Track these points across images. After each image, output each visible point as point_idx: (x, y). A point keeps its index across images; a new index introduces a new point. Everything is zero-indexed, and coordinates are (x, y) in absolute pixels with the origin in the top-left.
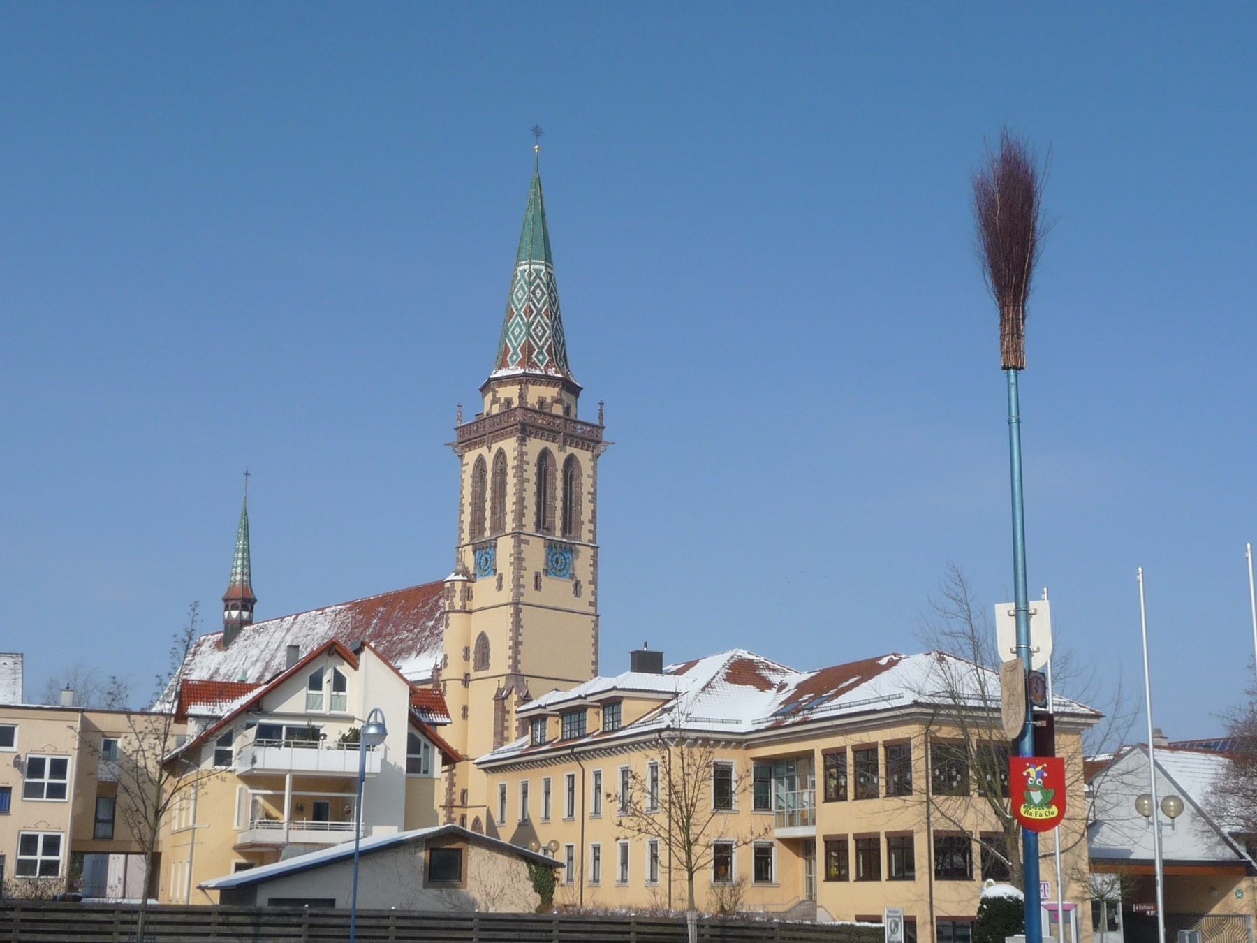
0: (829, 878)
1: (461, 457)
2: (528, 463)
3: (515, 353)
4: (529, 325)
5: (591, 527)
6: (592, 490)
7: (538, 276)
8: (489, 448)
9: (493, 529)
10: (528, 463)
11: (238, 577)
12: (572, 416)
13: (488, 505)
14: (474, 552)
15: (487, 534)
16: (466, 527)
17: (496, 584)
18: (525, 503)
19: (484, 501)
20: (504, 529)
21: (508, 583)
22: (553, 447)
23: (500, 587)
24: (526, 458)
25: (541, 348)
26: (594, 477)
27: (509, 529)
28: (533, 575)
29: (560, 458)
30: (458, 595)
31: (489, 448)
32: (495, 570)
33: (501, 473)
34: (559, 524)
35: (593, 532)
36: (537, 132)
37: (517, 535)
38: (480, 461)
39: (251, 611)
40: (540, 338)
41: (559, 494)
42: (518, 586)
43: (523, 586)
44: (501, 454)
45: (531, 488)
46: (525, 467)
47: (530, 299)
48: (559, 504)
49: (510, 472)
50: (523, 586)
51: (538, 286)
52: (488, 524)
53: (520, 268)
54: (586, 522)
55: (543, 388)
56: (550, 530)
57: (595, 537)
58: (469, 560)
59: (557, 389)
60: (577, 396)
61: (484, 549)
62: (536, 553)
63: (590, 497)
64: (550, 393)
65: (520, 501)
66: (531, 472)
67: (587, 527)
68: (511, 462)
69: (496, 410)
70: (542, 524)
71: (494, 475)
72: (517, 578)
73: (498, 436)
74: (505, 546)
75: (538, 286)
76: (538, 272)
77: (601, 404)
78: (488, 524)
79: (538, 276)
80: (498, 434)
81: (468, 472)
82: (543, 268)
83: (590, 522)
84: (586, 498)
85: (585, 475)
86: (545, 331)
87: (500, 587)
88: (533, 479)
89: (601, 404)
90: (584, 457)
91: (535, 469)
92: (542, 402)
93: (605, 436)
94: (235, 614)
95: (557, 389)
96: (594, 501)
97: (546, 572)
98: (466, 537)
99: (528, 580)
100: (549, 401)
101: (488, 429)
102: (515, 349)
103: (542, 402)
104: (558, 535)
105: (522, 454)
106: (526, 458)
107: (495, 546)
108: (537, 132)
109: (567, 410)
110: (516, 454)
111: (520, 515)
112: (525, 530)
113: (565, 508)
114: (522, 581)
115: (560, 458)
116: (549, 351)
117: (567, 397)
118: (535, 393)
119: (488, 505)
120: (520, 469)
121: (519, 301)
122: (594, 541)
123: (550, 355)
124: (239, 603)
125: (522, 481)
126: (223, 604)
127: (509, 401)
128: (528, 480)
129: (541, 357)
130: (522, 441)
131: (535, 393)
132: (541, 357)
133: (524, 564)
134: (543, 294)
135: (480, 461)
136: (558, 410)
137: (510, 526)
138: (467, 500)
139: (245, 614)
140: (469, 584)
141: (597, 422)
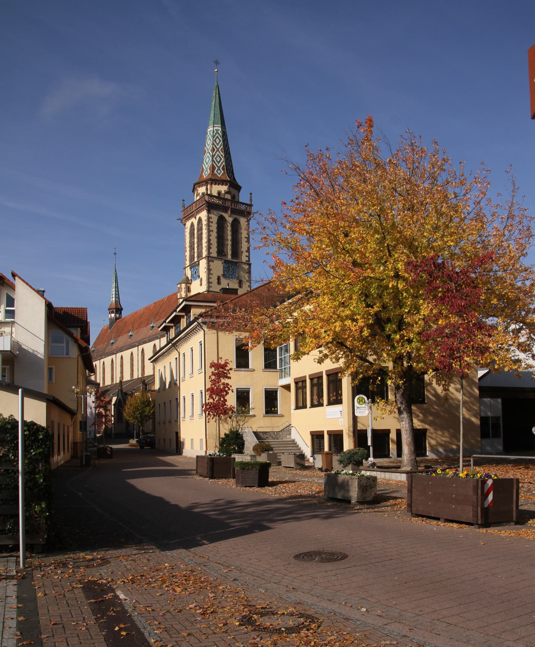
0: (297, 408)
1: (185, 225)
2: (212, 222)
3: (207, 171)
4: (213, 156)
5: (247, 254)
6: (247, 236)
7: (217, 133)
8: (195, 218)
9: (198, 257)
10: (212, 222)
11: (114, 299)
12: (236, 200)
13: (196, 245)
14: (191, 268)
15: (196, 260)
16: (188, 258)
17: (199, 283)
18: (211, 242)
19: (194, 244)
20: (202, 256)
21: (205, 282)
22: (226, 216)
23: (201, 285)
24: (211, 220)
25: (219, 167)
26: (248, 229)
27: (204, 256)
28: (216, 278)
29: (230, 220)
30: (183, 290)
31: (195, 218)
32: (199, 276)
33: (200, 229)
34: (230, 252)
35: (249, 257)
36: (217, 63)
37: (210, 259)
38: (192, 225)
39: (121, 314)
40: (219, 162)
41: (229, 237)
42: (209, 283)
43: (211, 283)
44: (200, 220)
45: (214, 235)
46: (211, 224)
47: (213, 144)
48: (229, 243)
49: (204, 227)
50: (211, 283)
51: (217, 137)
52: (196, 255)
53: (209, 130)
54: (244, 252)
55: (220, 186)
56: (226, 255)
57: (249, 259)
58: (189, 272)
59: (227, 187)
60: (239, 192)
61: (194, 266)
62: (218, 267)
63: (246, 240)
64: (223, 188)
65: (209, 241)
66: (214, 227)
67: (245, 254)
68: (204, 222)
69: (198, 198)
70: (221, 252)
71: (198, 231)
72: (209, 278)
73: (198, 212)
74: (203, 263)
75: (217, 137)
76: (217, 130)
77: (251, 194)
78: (196, 255)
79: (217, 133)
80: (198, 211)
81: (187, 231)
82: (220, 128)
83: (246, 251)
84: (244, 240)
85: (243, 229)
86: (221, 159)
87: (201, 285)
88: (215, 230)
89: (251, 194)
90: (243, 221)
91: (216, 226)
92: (219, 193)
93: (254, 210)
94: (113, 315)
95: (227, 187)
96: (248, 241)
97: (224, 275)
98: (188, 263)
99: (214, 280)
100: (223, 192)
101: (194, 209)
102: (206, 169)
103: (219, 193)
104: (229, 257)
105: (209, 218)
106: (211, 220)
107: (199, 264)
108: (217, 63)
109: (233, 197)
110: (206, 218)
111: (209, 248)
112: (211, 255)
113: (233, 245)
114: (210, 280)
115: (230, 220)
116: (223, 169)
117: (234, 191)
118: (216, 189)
119: (196, 245)
120: (208, 225)
121: (208, 145)
122: (249, 260)
123: (224, 170)
124: (114, 310)
125: (209, 231)
126: (108, 311)
127: (203, 194)
128: (212, 231)
129: (219, 172)
130: (209, 212)
131: (216, 189)
132: (219, 172)
133: (212, 272)
134: (220, 141)
135: (192, 225)
136: (228, 197)
137: (205, 253)
138: (188, 245)
139: (118, 316)
140: (188, 285)
141: (249, 203)
